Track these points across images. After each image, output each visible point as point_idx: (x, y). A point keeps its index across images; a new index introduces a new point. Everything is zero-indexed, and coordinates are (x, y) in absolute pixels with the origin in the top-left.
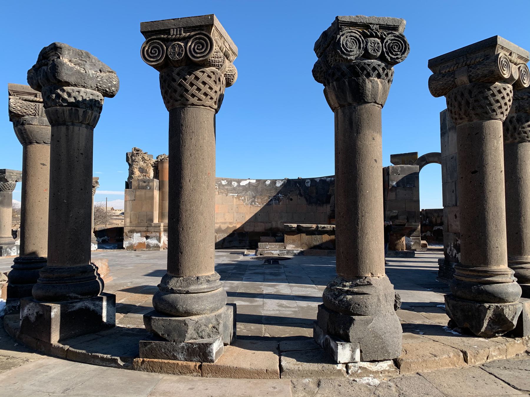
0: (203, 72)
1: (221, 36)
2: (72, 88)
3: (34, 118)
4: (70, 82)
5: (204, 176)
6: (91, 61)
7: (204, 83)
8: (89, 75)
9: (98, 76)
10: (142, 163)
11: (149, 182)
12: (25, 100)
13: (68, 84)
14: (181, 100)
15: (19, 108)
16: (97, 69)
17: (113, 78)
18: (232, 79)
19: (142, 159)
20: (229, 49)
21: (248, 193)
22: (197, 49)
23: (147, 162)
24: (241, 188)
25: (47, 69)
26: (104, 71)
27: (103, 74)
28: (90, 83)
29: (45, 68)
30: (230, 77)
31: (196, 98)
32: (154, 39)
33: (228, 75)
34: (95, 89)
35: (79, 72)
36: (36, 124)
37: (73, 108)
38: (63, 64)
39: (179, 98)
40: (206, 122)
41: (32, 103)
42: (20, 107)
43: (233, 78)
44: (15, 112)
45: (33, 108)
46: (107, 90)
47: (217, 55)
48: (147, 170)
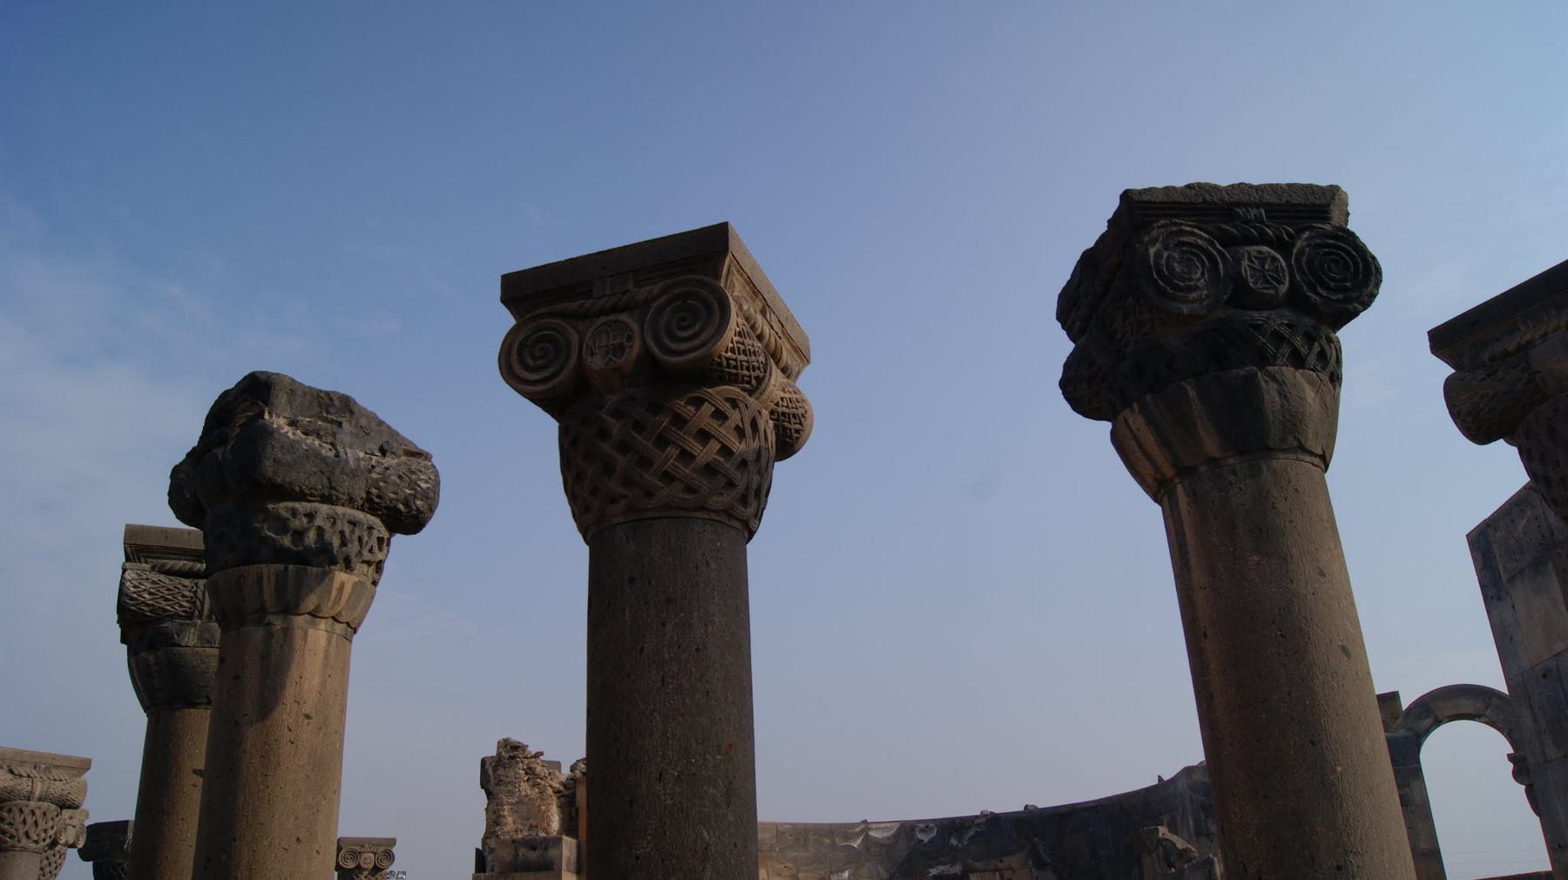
0: (699, 402)
1: (754, 292)
2: (291, 504)
3: (188, 624)
4: (287, 485)
5: (714, 758)
6: (357, 423)
7: (704, 436)
8: (347, 461)
9: (373, 467)
11: (546, 849)
12: (170, 573)
13: (285, 492)
14: (626, 497)
15: (146, 596)
16: (372, 446)
17: (421, 471)
18: (797, 431)
19: (526, 773)
20: (780, 334)
22: (681, 328)
23: (543, 782)
25: (223, 454)
26: (394, 450)
27: (389, 461)
28: (345, 486)
29: (219, 452)
30: (790, 422)
32: (541, 316)
33: (784, 414)
34: (362, 506)
35: (317, 454)
36: (191, 643)
37: (291, 567)
38: (268, 433)
39: (621, 490)
40: (713, 566)
41: (187, 582)
42: (150, 593)
43: (798, 426)
44: (133, 608)
45: (187, 593)
46: (401, 506)
47: (743, 344)
48: (543, 808)
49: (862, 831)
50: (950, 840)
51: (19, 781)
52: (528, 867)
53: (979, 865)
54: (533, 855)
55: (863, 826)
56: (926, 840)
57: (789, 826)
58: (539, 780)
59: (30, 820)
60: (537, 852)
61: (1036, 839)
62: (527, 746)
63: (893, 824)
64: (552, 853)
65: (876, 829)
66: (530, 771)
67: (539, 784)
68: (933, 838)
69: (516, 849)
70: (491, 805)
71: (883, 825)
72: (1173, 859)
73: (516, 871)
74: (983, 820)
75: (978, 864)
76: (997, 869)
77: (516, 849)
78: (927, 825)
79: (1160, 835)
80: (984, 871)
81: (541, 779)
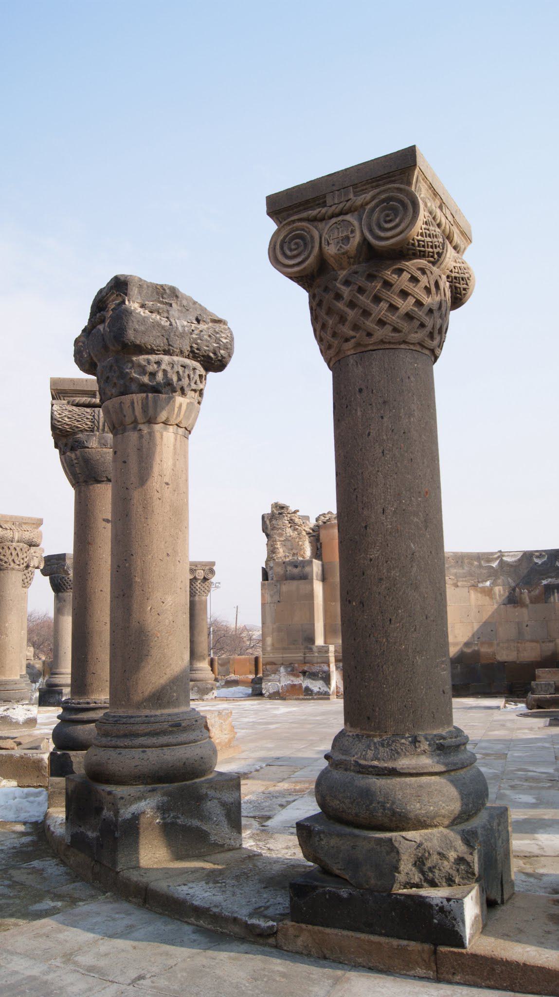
0: (400, 271)
1: (434, 194)
2: (146, 357)
3: (92, 435)
4: (143, 345)
5: (417, 499)
6: (181, 304)
7: (404, 294)
8: (177, 328)
9: (193, 331)
10: (289, 531)
11: (303, 567)
12: (78, 405)
13: (141, 350)
14: (355, 337)
15: (66, 419)
16: (191, 318)
17: (222, 332)
18: (464, 289)
19: (290, 523)
20: (452, 223)
21: (500, 581)
22: (386, 222)
23: (300, 528)
24: (485, 571)
25: (104, 329)
26: (204, 319)
27: (202, 326)
28: (177, 343)
29: (101, 327)
30: (459, 283)
31: (388, 328)
32: (293, 222)
33: (455, 278)
34: (188, 355)
35: (159, 325)
36: (94, 446)
37: (150, 395)
38: (128, 313)
39: (352, 333)
40: (412, 379)
41: (88, 410)
42: (69, 418)
43: (465, 286)
44: (60, 427)
45: (89, 417)
46: (212, 355)
47: (428, 230)
48: (300, 543)
49: (499, 557)
51: (5, 532)
52: (293, 578)
55: (499, 554)
56: (540, 563)
58: (297, 527)
59: (14, 553)
62: (289, 507)
64: (307, 569)
65: (507, 556)
66: (291, 521)
67: (297, 529)
68: (545, 561)
70: (269, 542)
71: (511, 554)
78: (541, 554)
81: (299, 526)
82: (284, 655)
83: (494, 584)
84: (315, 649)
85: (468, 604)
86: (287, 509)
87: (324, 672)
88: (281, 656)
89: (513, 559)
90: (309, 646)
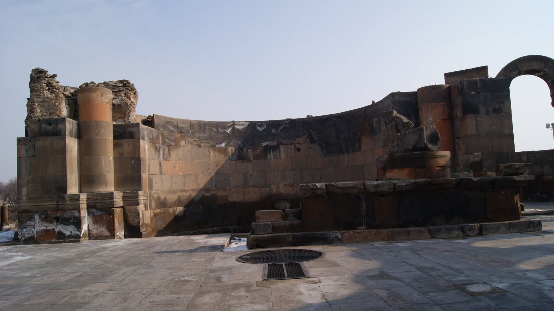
10: (47, 93)
11: (57, 124)
19: (47, 86)
21: (232, 143)
23: (57, 91)
24: (221, 136)
48: (57, 104)
49: (232, 125)
50: (272, 130)
52: (47, 134)
53: (284, 141)
54: (50, 128)
55: (232, 123)
56: (261, 130)
57: (196, 122)
58: (55, 90)
60: (52, 126)
61: (311, 130)
62: (47, 71)
63: (246, 123)
64: (60, 126)
65: (238, 125)
66: (49, 84)
67: (55, 92)
68: (264, 129)
69: (40, 125)
70: (29, 103)
71: (240, 123)
72: (400, 128)
73: (41, 136)
74: (288, 122)
75: (284, 141)
76: (292, 144)
77: (40, 125)
78: (262, 123)
79: (394, 115)
80: (287, 144)
81: (56, 89)
82: (39, 204)
83: (228, 145)
84: (67, 198)
85: (209, 160)
86: (46, 74)
87: (75, 218)
88: (36, 204)
89: (242, 127)
90: (62, 195)
